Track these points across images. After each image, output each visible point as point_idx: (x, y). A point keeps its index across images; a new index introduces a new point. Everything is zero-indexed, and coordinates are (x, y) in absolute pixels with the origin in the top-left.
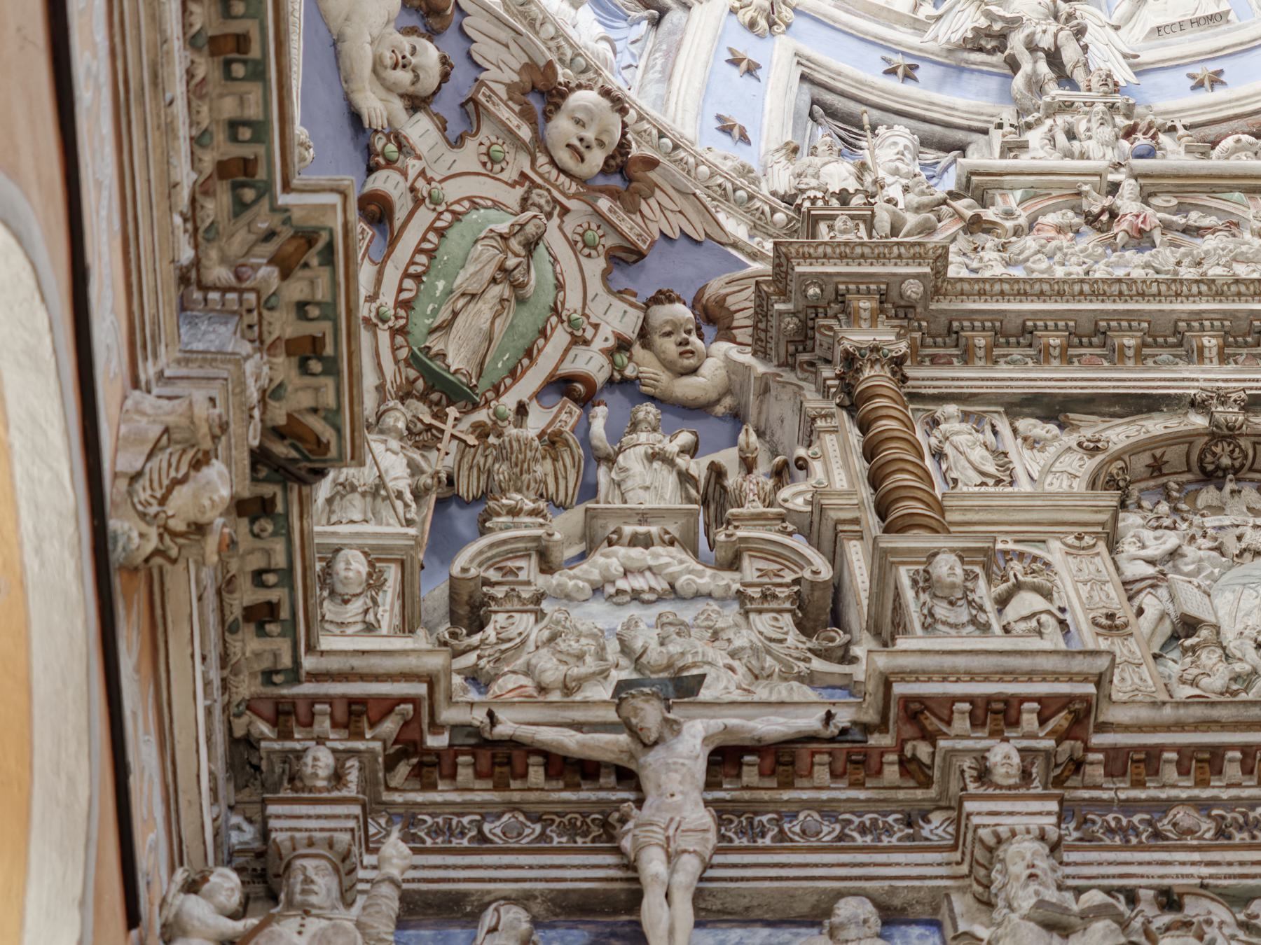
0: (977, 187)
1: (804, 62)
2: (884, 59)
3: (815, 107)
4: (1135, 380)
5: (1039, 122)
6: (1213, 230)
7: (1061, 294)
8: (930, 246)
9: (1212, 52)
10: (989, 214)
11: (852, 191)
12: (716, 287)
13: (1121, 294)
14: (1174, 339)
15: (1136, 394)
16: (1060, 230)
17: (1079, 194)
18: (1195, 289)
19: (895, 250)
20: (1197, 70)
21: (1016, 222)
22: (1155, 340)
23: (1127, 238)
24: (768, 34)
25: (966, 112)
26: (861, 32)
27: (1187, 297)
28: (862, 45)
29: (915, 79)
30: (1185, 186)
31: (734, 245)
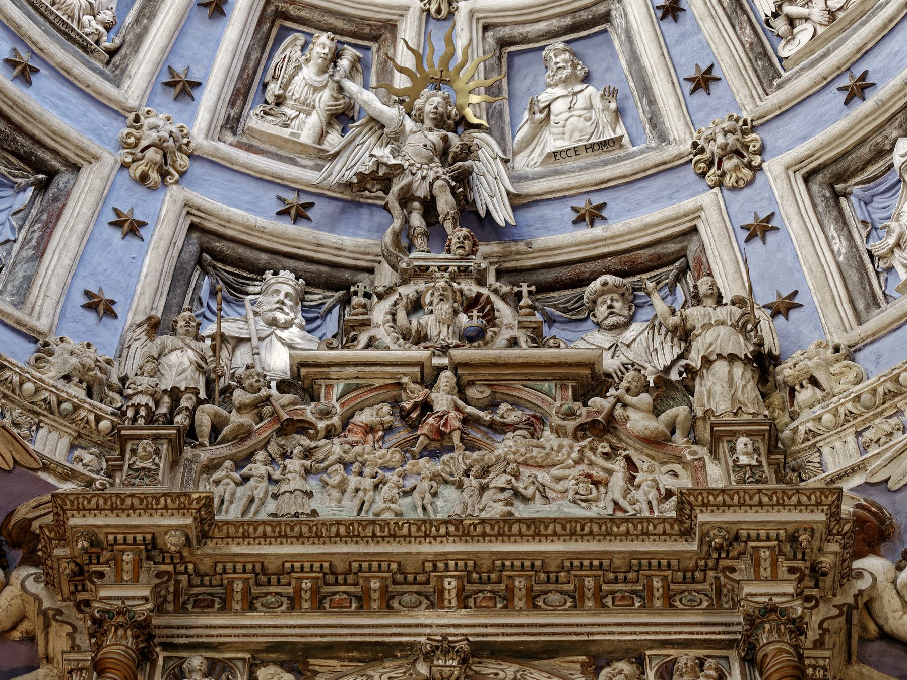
0: (306, 377)
1: (194, 212)
2: (279, 198)
3: (205, 255)
4: (373, 626)
5: (390, 291)
6: (514, 427)
7: (319, 536)
8: (195, 496)
9: (596, 185)
10: (309, 412)
11: (183, 389)
12: (23, 511)
13: (374, 535)
14: (413, 584)
15: (370, 642)
16: (369, 429)
17: (399, 385)
18: (443, 530)
19: (162, 500)
20: (581, 203)
21: (329, 422)
22: (405, 578)
23: (426, 441)
24: (160, 186)
25: (352, 252)
26: (259, 172)
27: (435, 538)
28: (261, 184)
29: (308, 219)
30: (501, 377)
31: (46, 468)
